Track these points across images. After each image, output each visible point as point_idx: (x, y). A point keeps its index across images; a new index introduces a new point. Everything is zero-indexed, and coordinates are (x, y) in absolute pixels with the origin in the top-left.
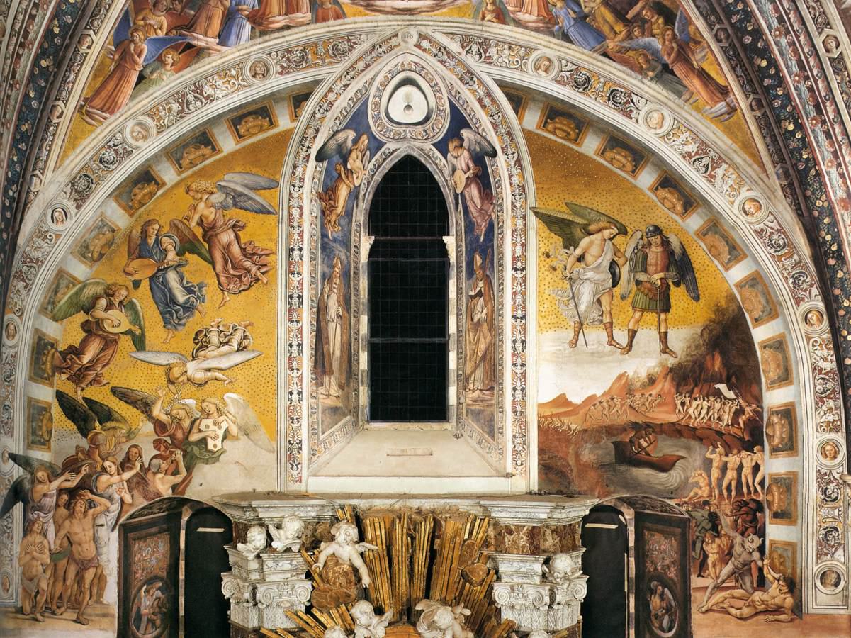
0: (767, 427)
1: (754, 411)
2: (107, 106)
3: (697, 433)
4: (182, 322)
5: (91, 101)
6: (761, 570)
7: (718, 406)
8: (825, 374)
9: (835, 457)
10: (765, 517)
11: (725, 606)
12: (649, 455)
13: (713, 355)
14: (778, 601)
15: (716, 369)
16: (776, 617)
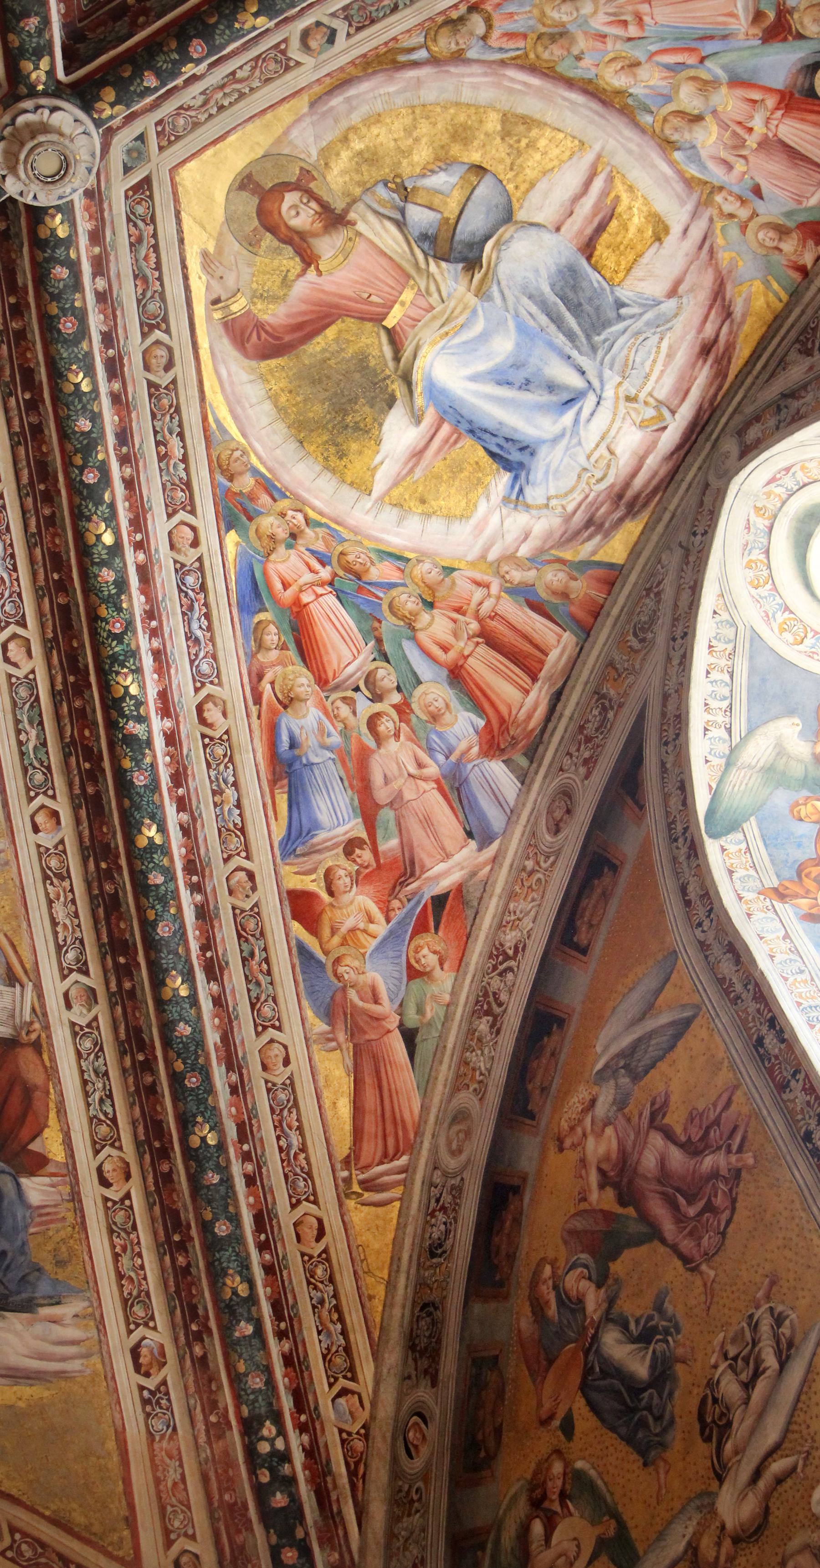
2: (391, 1141)
4: (667, 1417)
5: (357, 1158)
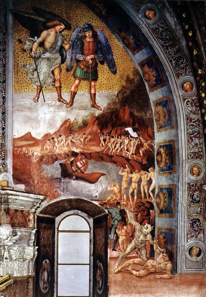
0: (157, 156)
1: (149, 145)
3: (114, 159)
6: (152, 246)
7: (126, 141)
8: (193, 122)
9: (198, 175)
10: (155, 213)
11: (129, 269)
12: (83, 173)
14: (162, 265)
15: (126, 118)
16: (161, 276)
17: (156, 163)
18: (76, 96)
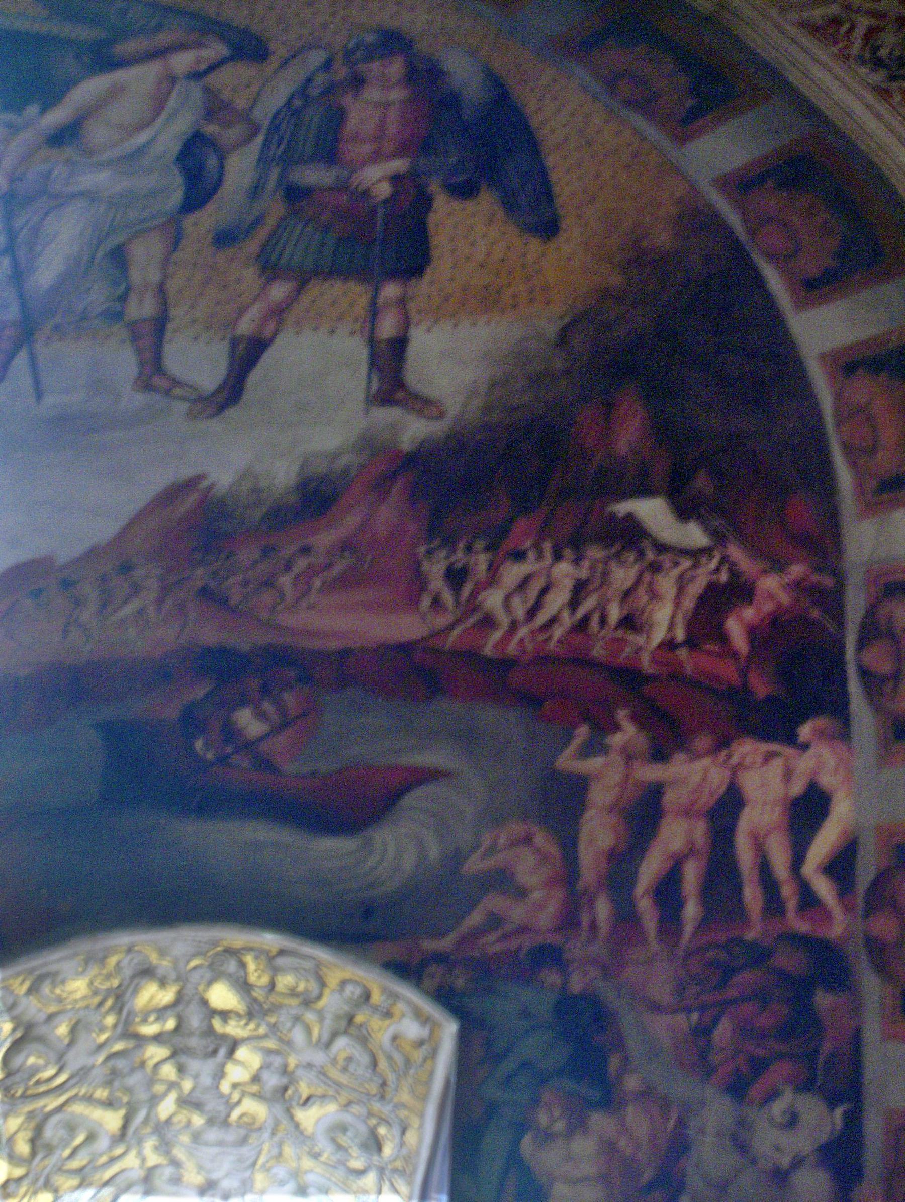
1: (797, 586)
10: (857, 1009)
13: (610, 406)
17: (854, 686)
18: (268, 357)
